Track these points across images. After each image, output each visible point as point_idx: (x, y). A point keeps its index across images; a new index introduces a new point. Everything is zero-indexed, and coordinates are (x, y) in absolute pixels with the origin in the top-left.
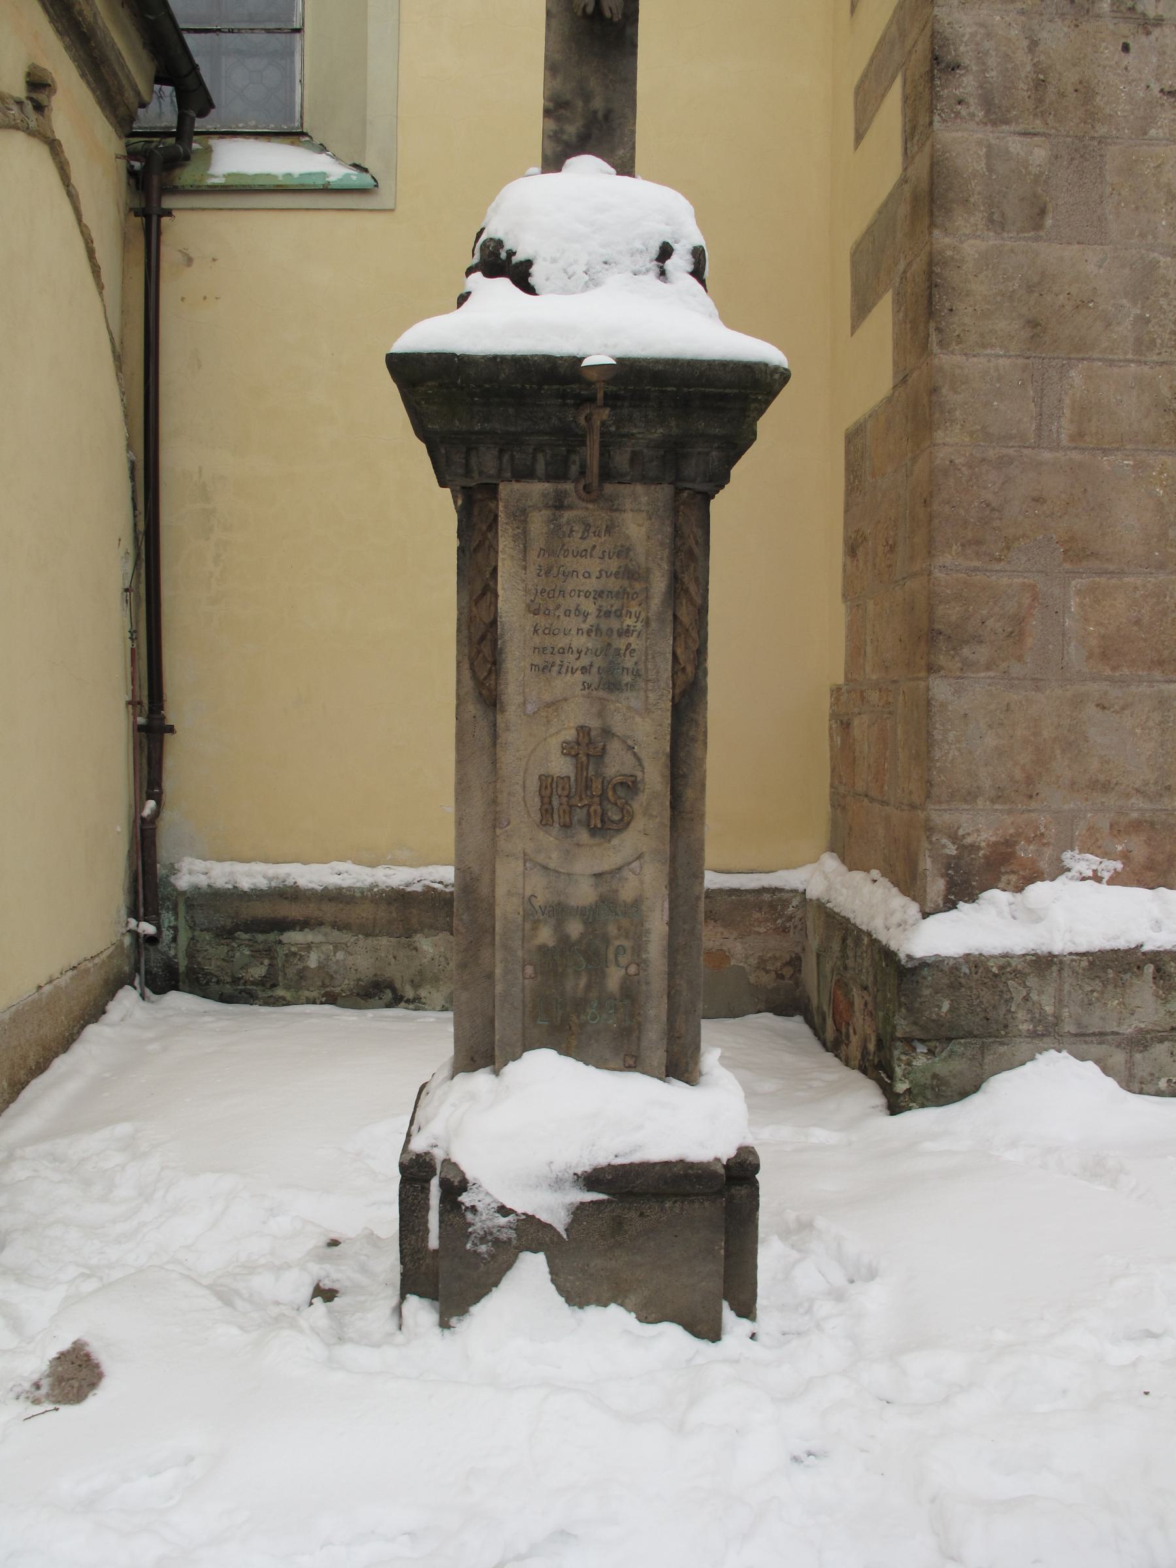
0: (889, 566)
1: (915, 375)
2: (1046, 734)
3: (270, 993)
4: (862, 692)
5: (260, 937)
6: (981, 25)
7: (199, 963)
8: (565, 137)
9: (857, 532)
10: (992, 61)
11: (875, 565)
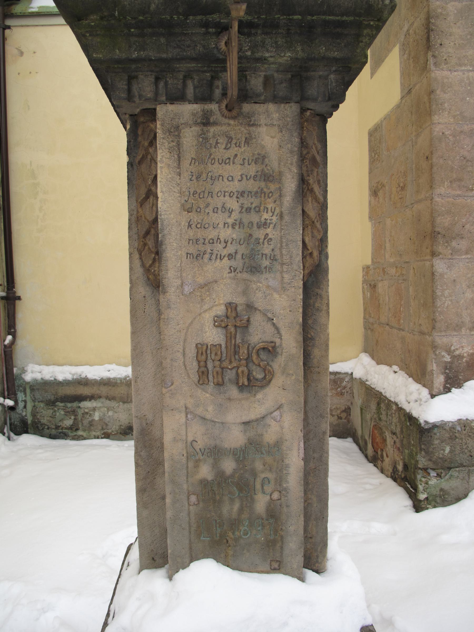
1: (417, 87)
3: (75, 433)
4: (383, 269)
5: (69, 405)
7: (38, 419)
9: (378, 183)
11: (390, 199)
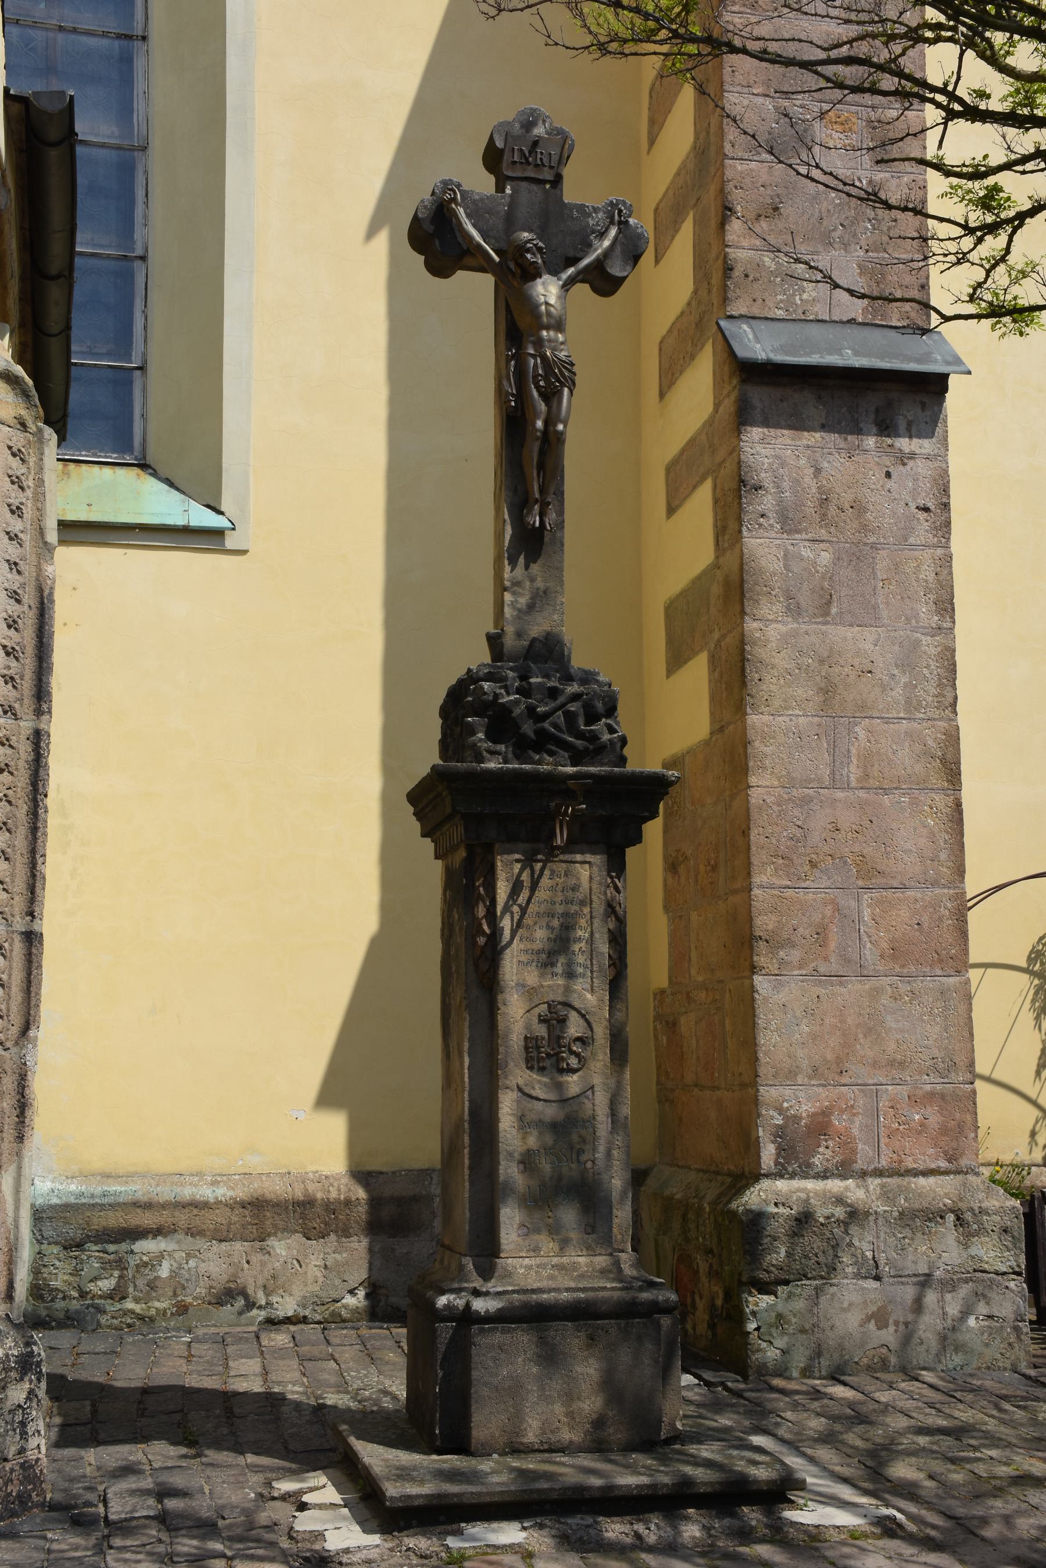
0: (711, 883)
1: (731, 727)
2: (849, 1021)
3: (118, 1306)
4: (688, 994)
5: (111, 1248)
6: (777, 457)
7: (45, 1279)
8: (519, 606)
9: (678, 851)
10: (786, 485)
11: (697, 881)
